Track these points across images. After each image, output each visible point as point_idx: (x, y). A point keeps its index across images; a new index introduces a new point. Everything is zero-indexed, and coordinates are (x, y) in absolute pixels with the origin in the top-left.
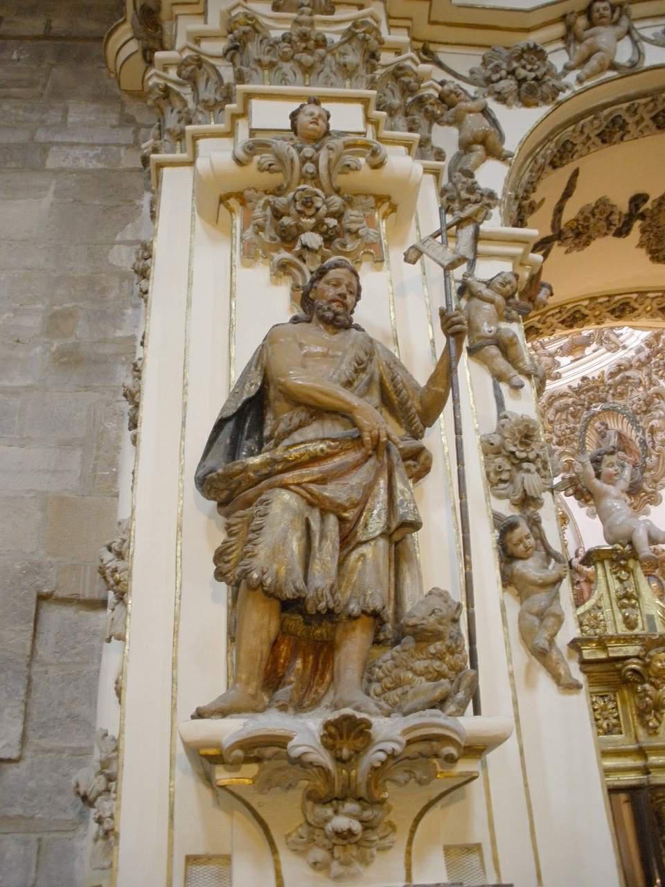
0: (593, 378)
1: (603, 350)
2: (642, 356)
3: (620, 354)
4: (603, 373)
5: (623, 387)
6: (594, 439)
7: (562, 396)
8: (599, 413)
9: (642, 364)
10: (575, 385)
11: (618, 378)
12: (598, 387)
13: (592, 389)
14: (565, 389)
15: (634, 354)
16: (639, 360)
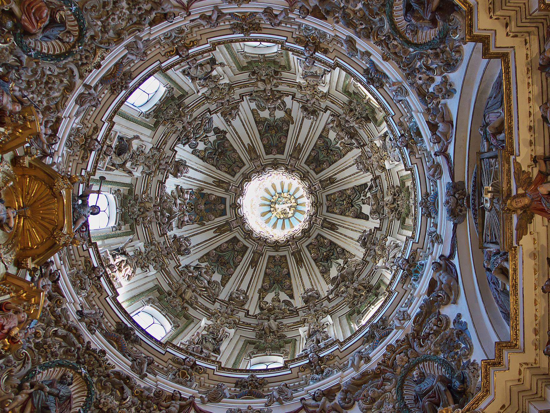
0: (107, 360)
1: (130, 363)
2: (146, 393)
3: (134, 376)
4: (113, 367)
5: (111, 386)
6: (54, 376)
7: (79, 337)
8: (81, 373)
9: (139, 394)
10: (93, 346)
11: (117, 380)
12: (100, 366)
13: (98, 361)
14: (87, 340)
15: (142, 387)
16: (142, 392)
